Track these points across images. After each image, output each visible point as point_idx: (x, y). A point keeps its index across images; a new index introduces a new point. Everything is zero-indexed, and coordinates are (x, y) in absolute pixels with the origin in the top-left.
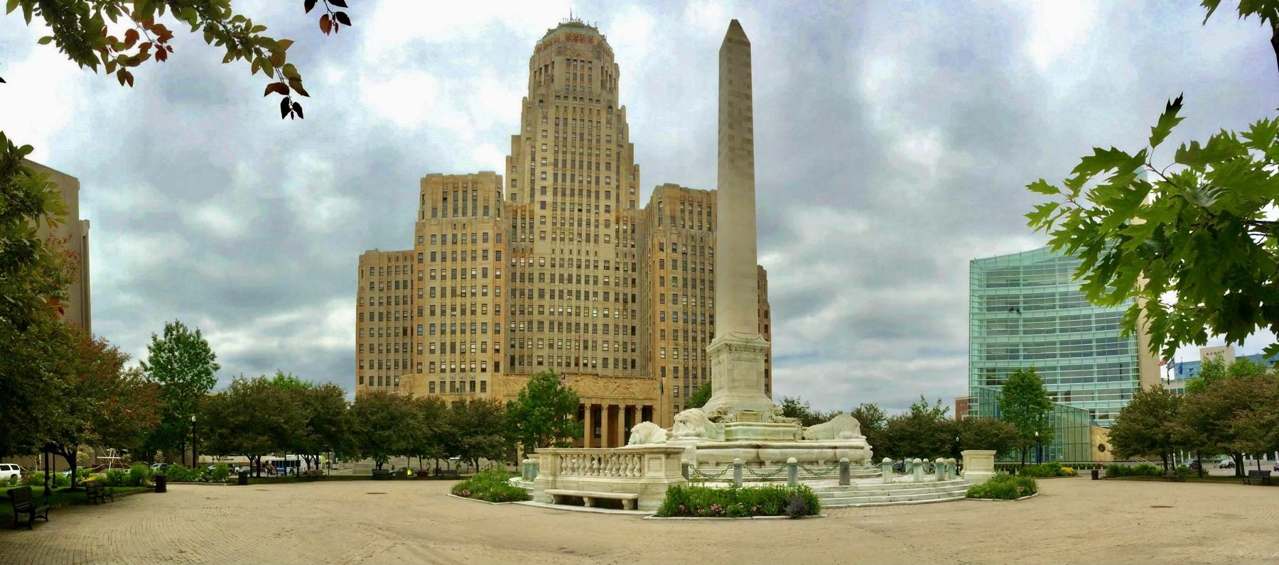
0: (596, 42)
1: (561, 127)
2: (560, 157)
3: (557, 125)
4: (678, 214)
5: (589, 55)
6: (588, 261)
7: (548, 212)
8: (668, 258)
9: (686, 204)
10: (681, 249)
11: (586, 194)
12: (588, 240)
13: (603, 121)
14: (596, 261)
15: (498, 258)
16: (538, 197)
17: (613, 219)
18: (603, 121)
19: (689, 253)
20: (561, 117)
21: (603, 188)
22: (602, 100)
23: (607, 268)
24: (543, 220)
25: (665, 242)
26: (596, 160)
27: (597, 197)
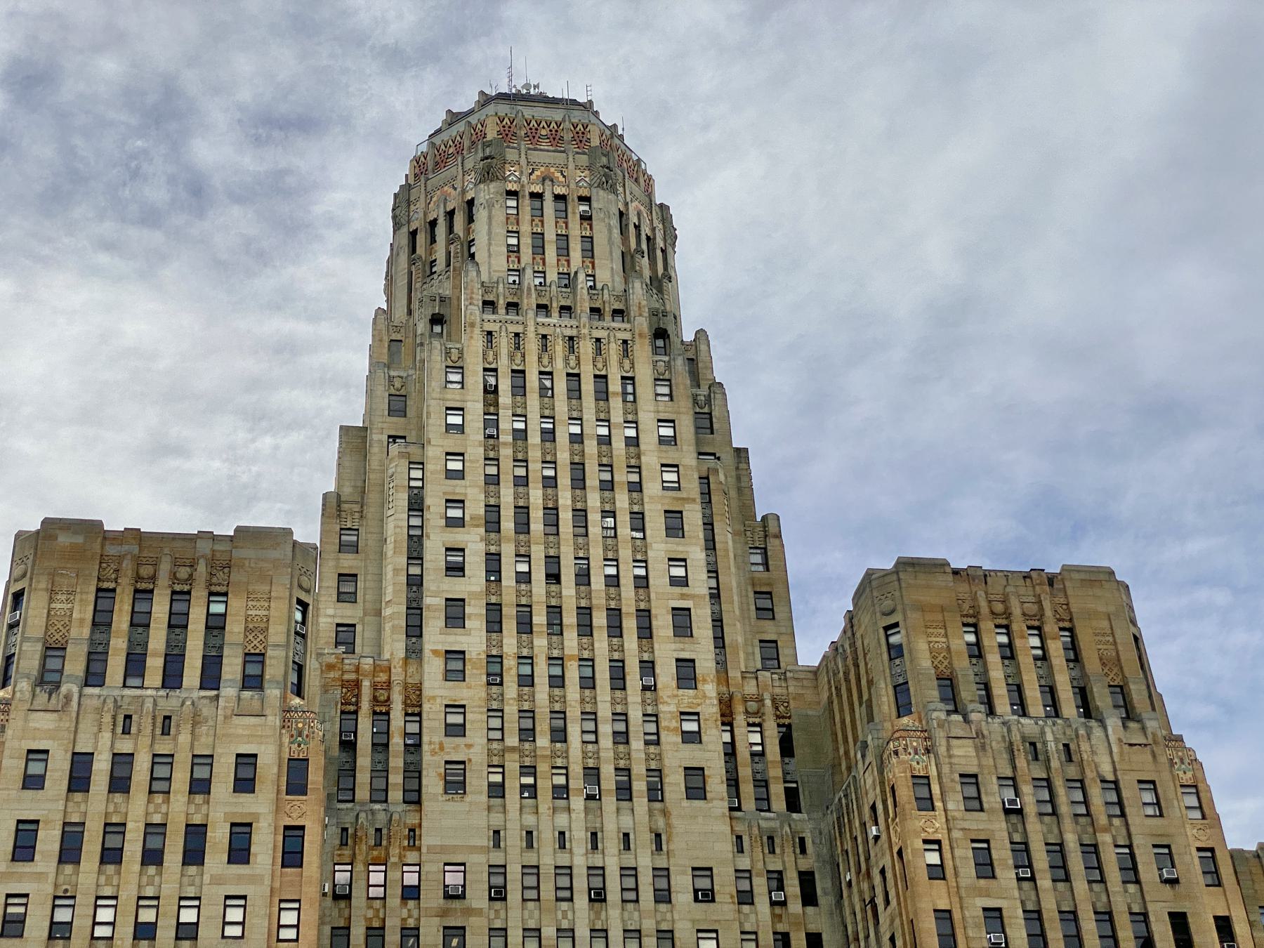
0: (595, 142)
1: (505, 398)
2: (507, 495)
3: (491, 392)
4: (963, 666)
5: (577, 178)
6: (629, 872)
7: (473, 691)
8: (956, 834)
9: (987, 625)
10: (994, 796)
11: (604, 622)
12: (625, 792)
13: (644, 374)
14: (662, 873)
15: (292, 856)
16: (436, 636)
17: (710, 710)
18: (644, 374)
19: (1031, 809)
20: (504, 365)
21: (663, 601)
22: (634, 311)
23: (705, 896)
24: (456, 719)
25: (933, 772)
26: (632, 503)
27: (646, 632)
